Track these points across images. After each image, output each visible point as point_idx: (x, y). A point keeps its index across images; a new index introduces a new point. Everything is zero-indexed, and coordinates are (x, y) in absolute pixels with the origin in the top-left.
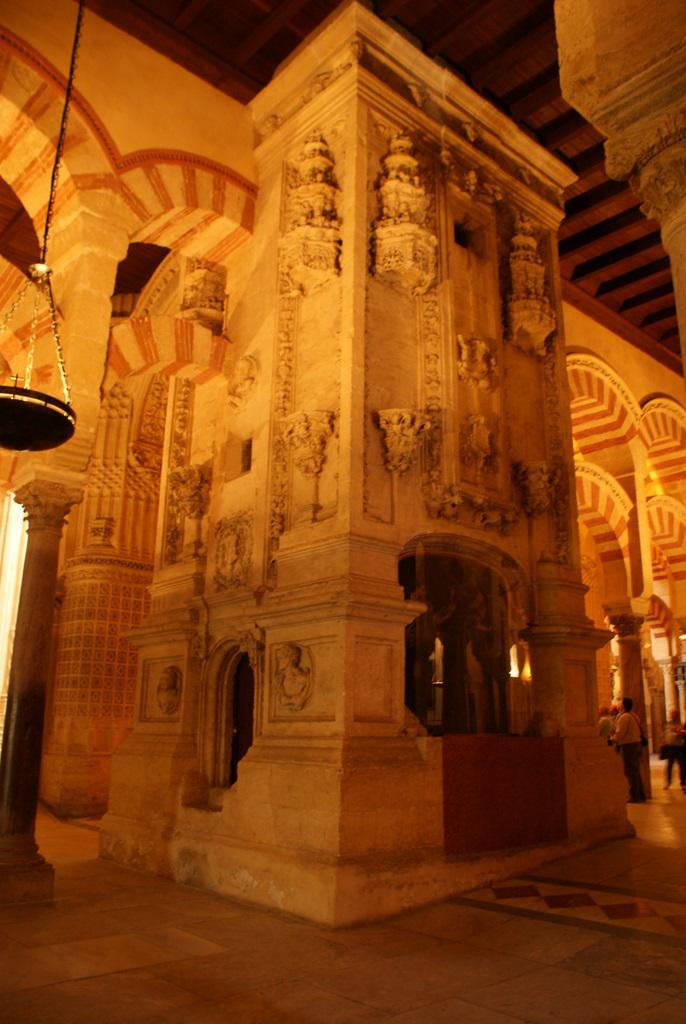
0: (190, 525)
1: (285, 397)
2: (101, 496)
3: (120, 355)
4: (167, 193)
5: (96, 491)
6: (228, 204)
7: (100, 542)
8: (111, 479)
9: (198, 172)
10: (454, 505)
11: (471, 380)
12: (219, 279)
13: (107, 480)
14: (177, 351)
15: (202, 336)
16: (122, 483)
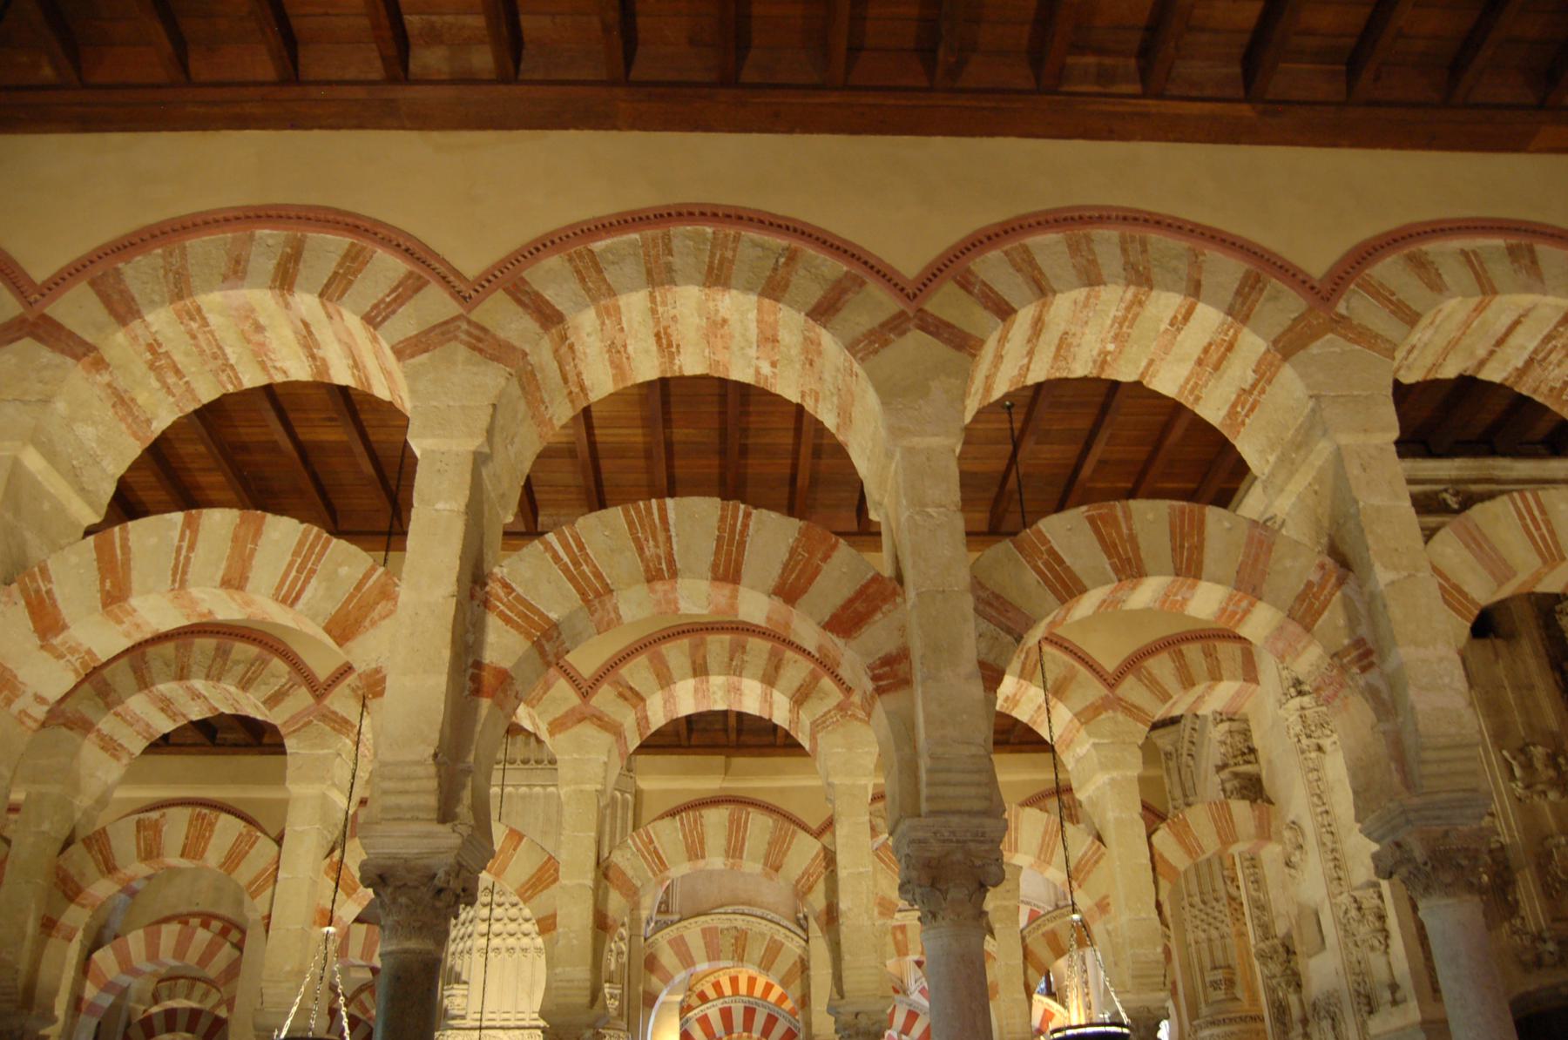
0: (1293, 999)
1: (1335, 867)
2: (1210, 940)
3: (1166, 862)
4: (1162, 687)
5: (1203, 936)
6: (1224, 665)
7: (1223, 997)
8: (1215, 918)
9: (1184, 648)
10: (1551, 953)
11: (1535, 797)
12: (1245, 726)
13: (1212, 921)
14: (1220, 837)
15: (1241, 809)
16: (1228, 920)
